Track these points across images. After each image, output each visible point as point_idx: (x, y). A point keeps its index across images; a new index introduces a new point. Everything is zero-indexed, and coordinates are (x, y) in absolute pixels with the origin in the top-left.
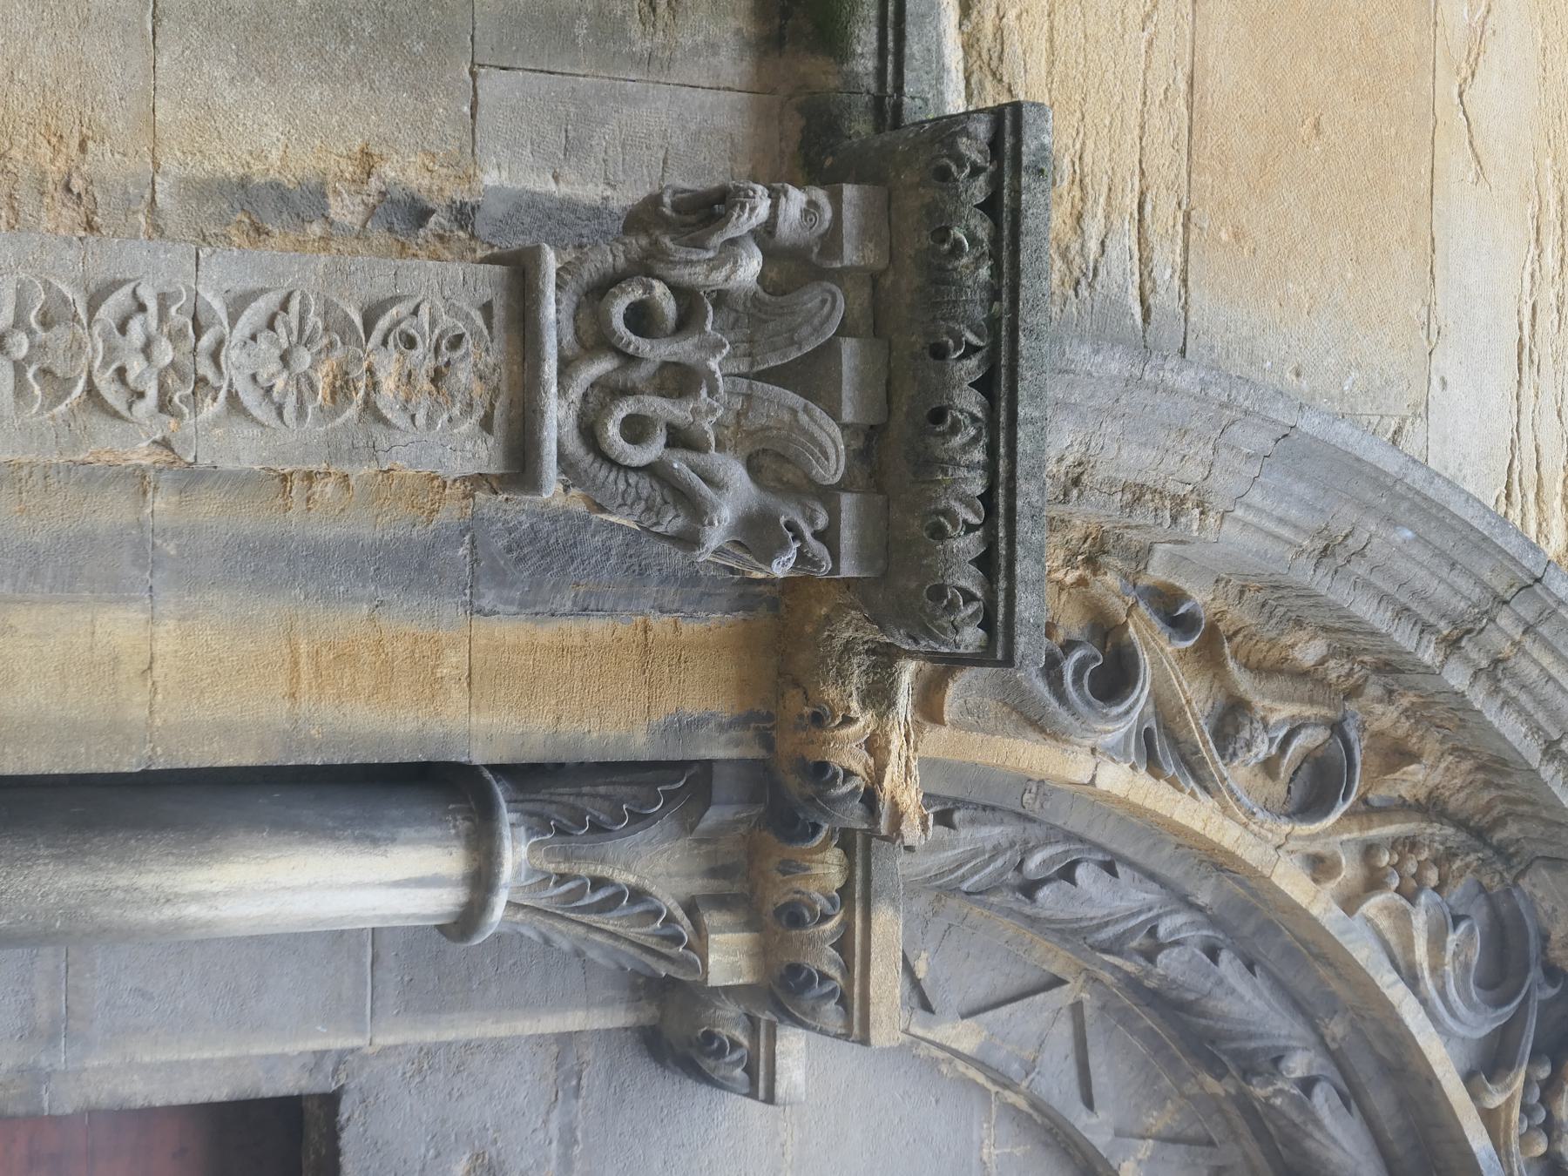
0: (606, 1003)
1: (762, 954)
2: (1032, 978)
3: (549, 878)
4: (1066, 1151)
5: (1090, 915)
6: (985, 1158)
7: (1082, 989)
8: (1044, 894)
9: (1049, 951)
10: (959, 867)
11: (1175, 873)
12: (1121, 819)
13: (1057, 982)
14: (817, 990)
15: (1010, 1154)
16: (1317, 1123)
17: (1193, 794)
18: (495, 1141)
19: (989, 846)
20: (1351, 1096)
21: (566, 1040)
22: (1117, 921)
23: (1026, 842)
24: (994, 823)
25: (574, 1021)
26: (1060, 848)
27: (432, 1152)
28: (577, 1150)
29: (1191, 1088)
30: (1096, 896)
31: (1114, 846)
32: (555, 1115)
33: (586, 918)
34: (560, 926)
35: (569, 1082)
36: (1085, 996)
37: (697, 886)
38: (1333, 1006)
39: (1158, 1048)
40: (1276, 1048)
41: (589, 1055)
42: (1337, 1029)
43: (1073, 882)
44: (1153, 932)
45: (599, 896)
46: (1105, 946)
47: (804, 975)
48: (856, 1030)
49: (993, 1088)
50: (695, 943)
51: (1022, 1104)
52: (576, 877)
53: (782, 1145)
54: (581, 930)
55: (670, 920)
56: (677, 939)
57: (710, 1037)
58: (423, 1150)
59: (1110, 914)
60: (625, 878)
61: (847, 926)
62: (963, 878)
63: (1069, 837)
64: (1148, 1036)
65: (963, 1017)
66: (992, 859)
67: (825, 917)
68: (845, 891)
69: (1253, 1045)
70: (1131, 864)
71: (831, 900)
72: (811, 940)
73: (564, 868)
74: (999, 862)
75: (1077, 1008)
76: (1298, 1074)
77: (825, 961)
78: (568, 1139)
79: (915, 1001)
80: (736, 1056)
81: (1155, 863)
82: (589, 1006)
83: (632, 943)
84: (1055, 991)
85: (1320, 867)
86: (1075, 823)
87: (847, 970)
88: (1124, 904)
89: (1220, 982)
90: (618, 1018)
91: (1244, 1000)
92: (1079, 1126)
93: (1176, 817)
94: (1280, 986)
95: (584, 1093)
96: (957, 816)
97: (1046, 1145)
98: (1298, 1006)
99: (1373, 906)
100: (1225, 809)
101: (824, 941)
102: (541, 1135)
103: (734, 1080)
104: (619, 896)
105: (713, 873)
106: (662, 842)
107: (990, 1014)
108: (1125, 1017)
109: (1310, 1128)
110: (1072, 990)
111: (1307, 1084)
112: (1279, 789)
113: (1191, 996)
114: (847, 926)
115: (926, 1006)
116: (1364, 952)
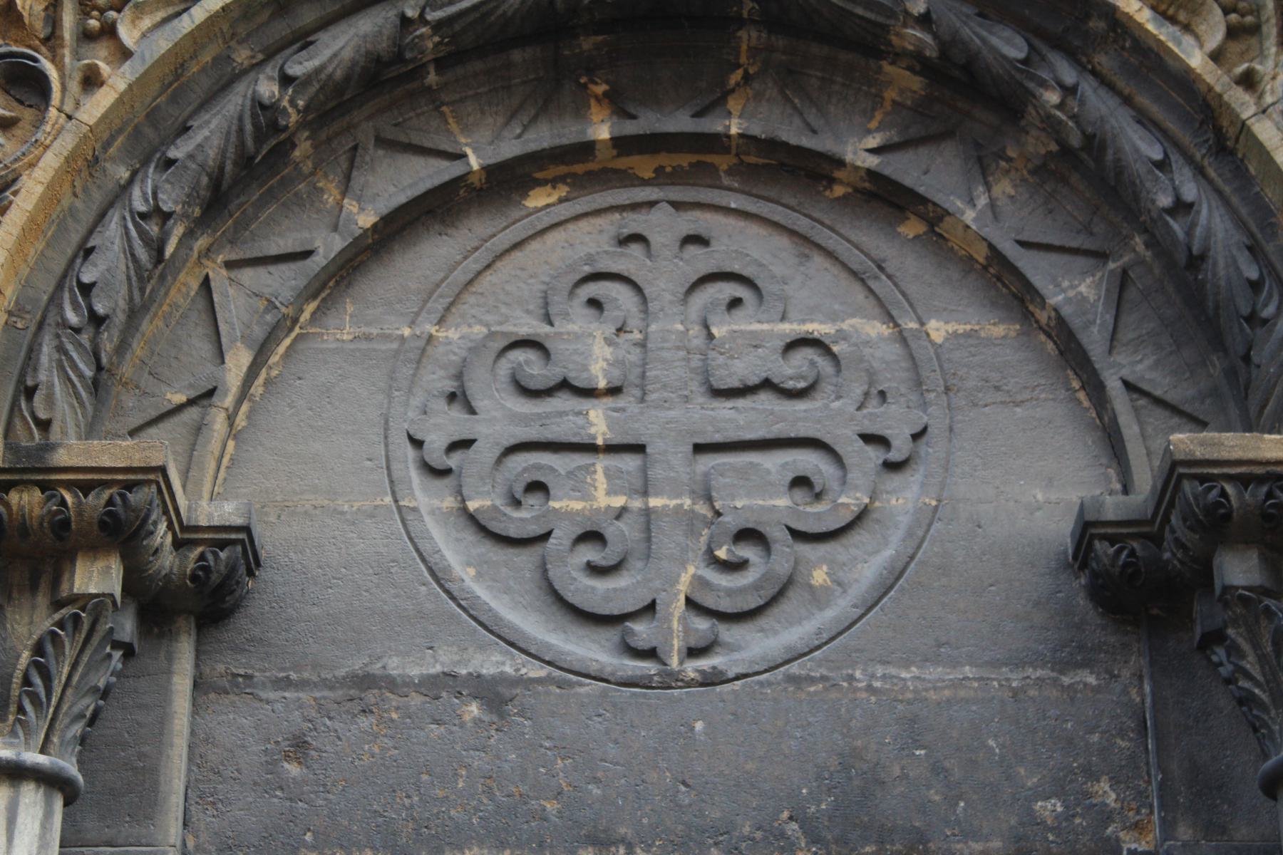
0: (170, 659)
1: (94, 549)
2: (201, 304)
3: (19, 720)
4: (355, 269)
5: (124, 269)
6: (351, 337)
7: (214, 261)
8: (100, 309)
9: (179, 290)
10: (70, 380)
11: (98, 197)
12: (48, 245)
13: (206, 283)
14: (119, 509)
15: (351, 316)
16: (318, 71)
17: (15, 193)
18: (277, 743)
19: (56, 356)
20: (303, 40)
21: (199, 685)
22: (131, 247)
23: (58, 324)
24: (40, 351)
25: (182, 684)
26: (66, 295)
27: (278, 793)
28: (293, 676)
29: (307, 167)
30: (108, 265)
31: (70, 252)
32: (263, 695)
33: (57, 691)
34: (65, 707)
35: (242, 684)
36: (220, 259)
37: (42, 600)
38: (223, 59)
39: (269, 197)
40: (253, 107)
41: (221, 668)
42: (242, 56)
43: (93, 284)
44: (143, 216)
45: (37, 680)
46: (154, 253)
47: (106, 518)
48: (152, 477)
49: (297, 330)
50: (81, 603)
51: (310, 308)
52: (20, 696)
53: (315, 507)
54: (69, 692)
55: (61, 624)
56: (76, 619)
57: (194, 577)
58: (275, 800)
59: (125, 253)
60: (25, 657)
61: (69, 485)
62: (81, 376)
63: (60, 287)
64: (262, 204)
65: (223, 362)
66: (66, 353)
67: (63, 503)
68: (44, 486)
69: (248, 127)
70: (90, 232)
71: (49, 498)
72: (80, 514)
73: (13, 708)
74: (70, 347)
75: (229, 265)
76: (276, 89)
77: (96, 502)
78: (286, 683)
79: (205, 402)
80: (210, 557)
81: (87, 218)
82: (169, 672)
83: (81, 651)
84: (213, 284)
85: (91, 81)
86: (45, 287)
87: (106, 484)
88: (117, 241)
89: (191, 156)
90: (185, 650)
91: (209, 135)
92: (324, 262)
93: (30, 208)
94: (206, 103)
95: (250, 672)
96: (30, 383)
97: (349, 285)
98: (225, 86)
99: (127, 34)
100: (32, 165)
101: (80, 503)
102: (278, 706)
103: (228, 558)
104: (36, 665)
105: (34, 588)
106: (5, 629)
107: (224, 340)
108: (242, 225)
109: (323, 76)
110: (213, 269)
111: (286, 80)
112: (28, 115)
113: (205, 180)
114: (69, 485)
115: (210, 393)
116: (163, 43)
